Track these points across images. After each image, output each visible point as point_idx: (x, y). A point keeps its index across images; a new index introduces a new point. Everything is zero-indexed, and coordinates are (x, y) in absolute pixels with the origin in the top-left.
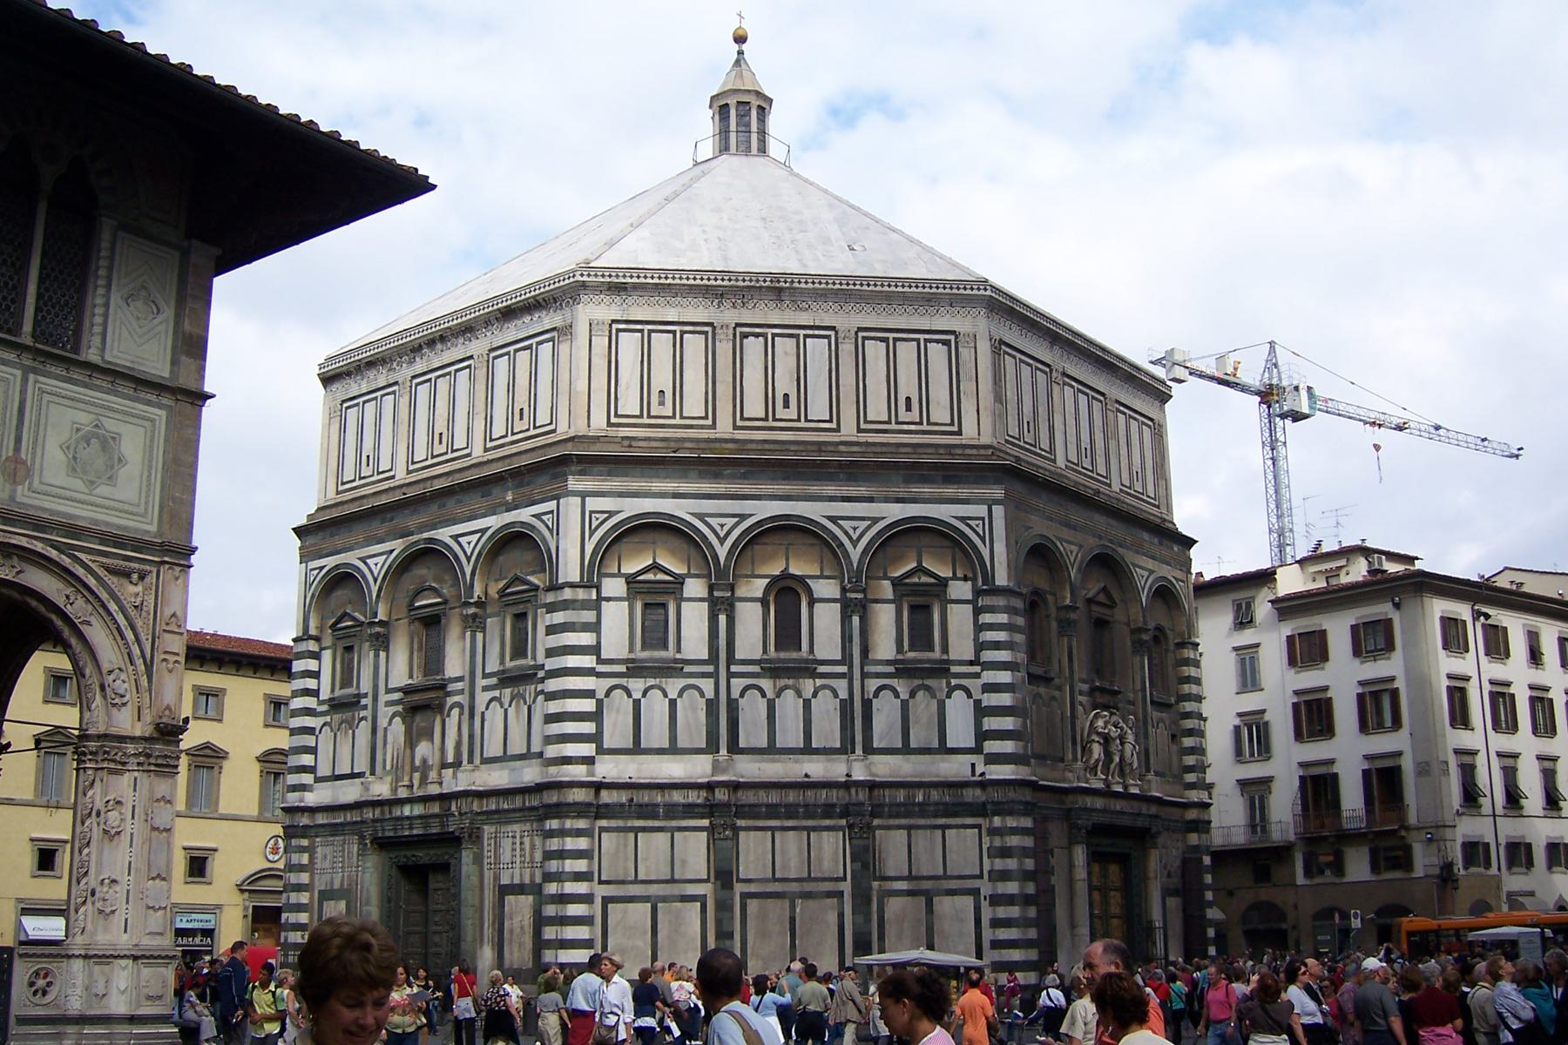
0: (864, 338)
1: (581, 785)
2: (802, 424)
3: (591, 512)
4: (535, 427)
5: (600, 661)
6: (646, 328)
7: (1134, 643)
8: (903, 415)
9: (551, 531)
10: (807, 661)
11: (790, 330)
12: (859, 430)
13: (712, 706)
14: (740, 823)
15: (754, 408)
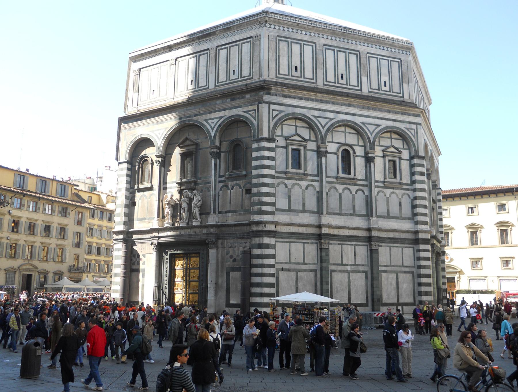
0: (369, 57)
1: (272, 223)
2: (348, 87)
3: (273, 110)
4: (241, 77)
5: (277, 172)
6: (289, 41)
7: (433, 185)
8: (384, 88)
9: (255, 118)
10: (353, 179)
11: (343, 50)
12: (369, 92)
13: (320, 194)
14: (331, 242)
15: (331, 77)
